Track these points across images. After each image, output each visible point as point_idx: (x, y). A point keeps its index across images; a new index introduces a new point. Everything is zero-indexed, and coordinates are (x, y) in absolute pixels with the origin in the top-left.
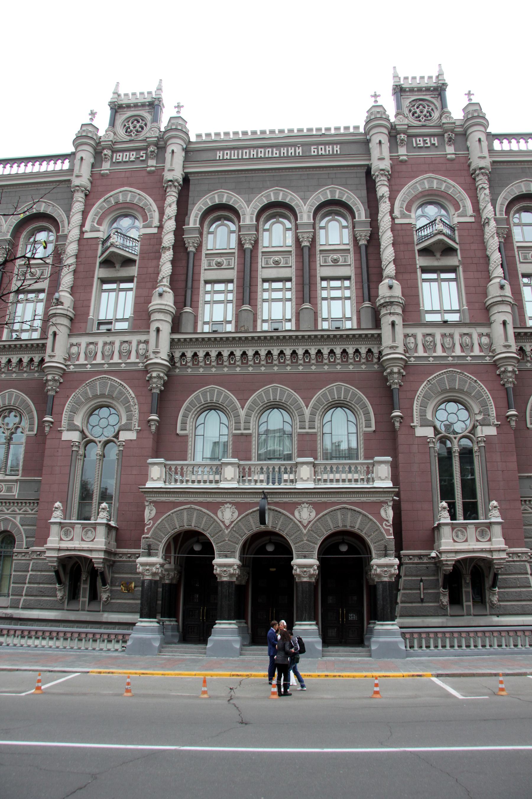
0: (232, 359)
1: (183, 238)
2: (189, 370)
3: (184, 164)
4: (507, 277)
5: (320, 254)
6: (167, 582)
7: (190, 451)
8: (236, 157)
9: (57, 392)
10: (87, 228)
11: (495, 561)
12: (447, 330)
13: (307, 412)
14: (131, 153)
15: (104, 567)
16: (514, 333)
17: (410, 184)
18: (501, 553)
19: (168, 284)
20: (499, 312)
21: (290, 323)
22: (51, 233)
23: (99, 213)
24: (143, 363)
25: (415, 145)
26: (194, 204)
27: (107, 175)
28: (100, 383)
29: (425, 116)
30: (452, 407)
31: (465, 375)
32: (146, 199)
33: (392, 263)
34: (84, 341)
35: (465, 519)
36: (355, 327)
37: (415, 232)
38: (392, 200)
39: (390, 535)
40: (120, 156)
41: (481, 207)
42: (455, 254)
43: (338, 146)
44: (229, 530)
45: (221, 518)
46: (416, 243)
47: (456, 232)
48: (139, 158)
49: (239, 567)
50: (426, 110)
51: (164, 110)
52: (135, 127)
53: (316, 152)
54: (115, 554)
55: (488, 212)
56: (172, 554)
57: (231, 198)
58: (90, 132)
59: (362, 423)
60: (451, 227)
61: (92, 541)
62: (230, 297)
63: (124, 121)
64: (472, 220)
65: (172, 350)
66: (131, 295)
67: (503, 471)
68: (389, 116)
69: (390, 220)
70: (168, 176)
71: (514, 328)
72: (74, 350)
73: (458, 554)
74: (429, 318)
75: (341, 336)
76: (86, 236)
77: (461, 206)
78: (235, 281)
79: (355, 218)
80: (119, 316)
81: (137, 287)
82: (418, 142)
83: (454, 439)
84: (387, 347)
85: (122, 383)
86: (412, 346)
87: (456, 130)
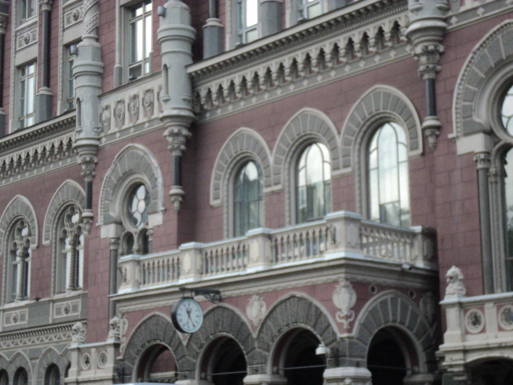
2: (219, 111)
72: (106, 114)
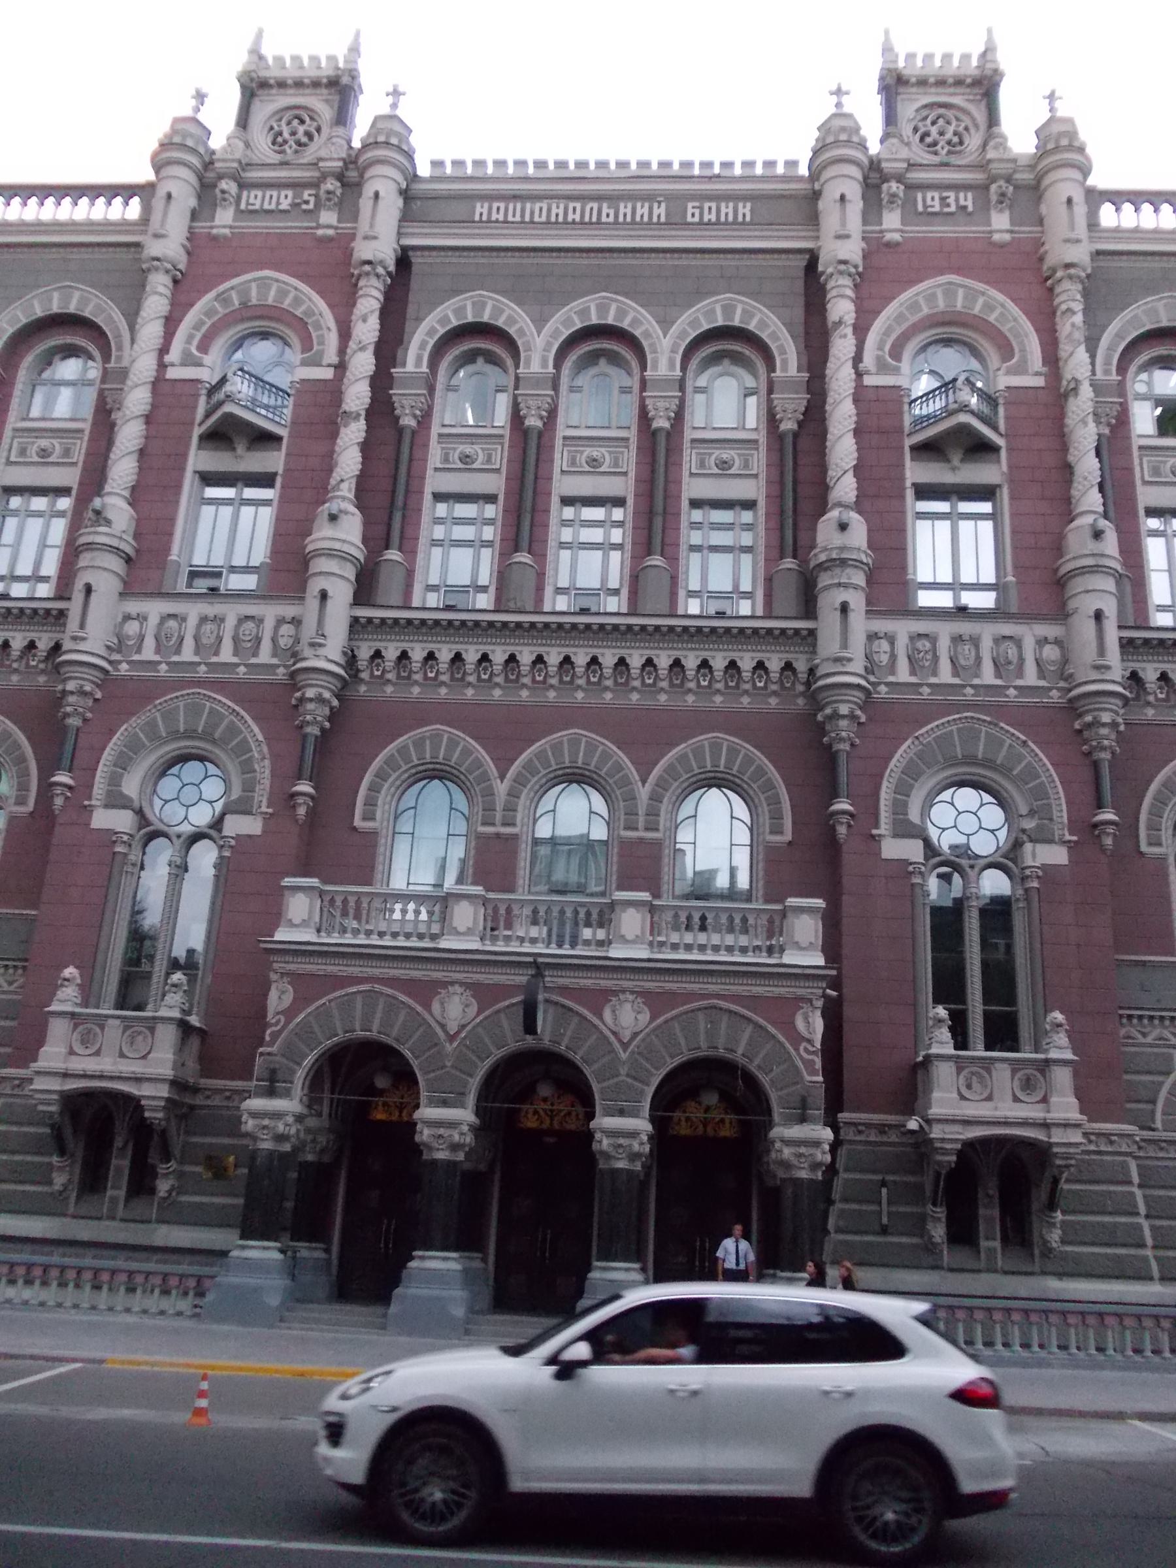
0: (485, 669)
1: (390, 396)
3: (400, 227)
4: (1111, 514)
5: (692, 448)
6: (310, 1157)
7: (380, 868)
8: (518, 218)
9: (85, 720)
10: (174, 355)
11: (1055, 1150)
12: (965, 628)
13: (643, 793)
14: (283, 193)
15: (168, 1119)
16: (1121, 639)
17: (904, 297)
18: (1069, 1131)
19: (351, 496)
20: (1087, 591)
21: (616, 599)
22: (90, 363)
23: (203, 323)
24: (285, 666)
25: (920, 208)
26: (419, 320)
27: (225, 237)
28: (185, 706)
29: (949, 143)
30: (967, 797)
31: (1002, 728)
32: (310, 300)
33: (851, 473)
34: (155, 609)
35: (987, 1048)
36: (760, 612)
37: (906, 407)
38: (861, 331)
39: (813, 1073)
40: (256, 197)
41: (1063, 354)
42: (994, 456)
43: (749, 205)
44: (455, 1044)
45: (439, 1018)
46: (907, 430)
47: (1001, 410)
48: (298, 205)
49: (473, 1128)
50: (951, 129)
51: (361, 98)
52: (293, 133)
53: (697, 215)
54: (196, 1090)
55: (1077, 363)
56: (327, 1095)
57: (502, 311)
58: (191, 136)
59: (764, 825)
60: (990, 397)
61: (144, 1057)
62: (488, 533)
63: (269, 118)
64: (1040, 382)
65: (354, 643)
66: (266, 515)
67: (1078, 945)
68: (865, 140)
69: (854, 376)
70: (363, 250)
71: (1120, 627)
72: (132, 628)
73: (969, 1128)
74: (926, 599)
75: (728, 630)
76: (172, 373)
77: (1017, 350)
78: (501, 498)
79: (774, 371)
80: (239, 560)
81: (283, 499)
82: (929, 202)
83: (968, 870)
84: (828, 659)
85: (237, 708)
86: (885, 659)
87: (1017, 176)
